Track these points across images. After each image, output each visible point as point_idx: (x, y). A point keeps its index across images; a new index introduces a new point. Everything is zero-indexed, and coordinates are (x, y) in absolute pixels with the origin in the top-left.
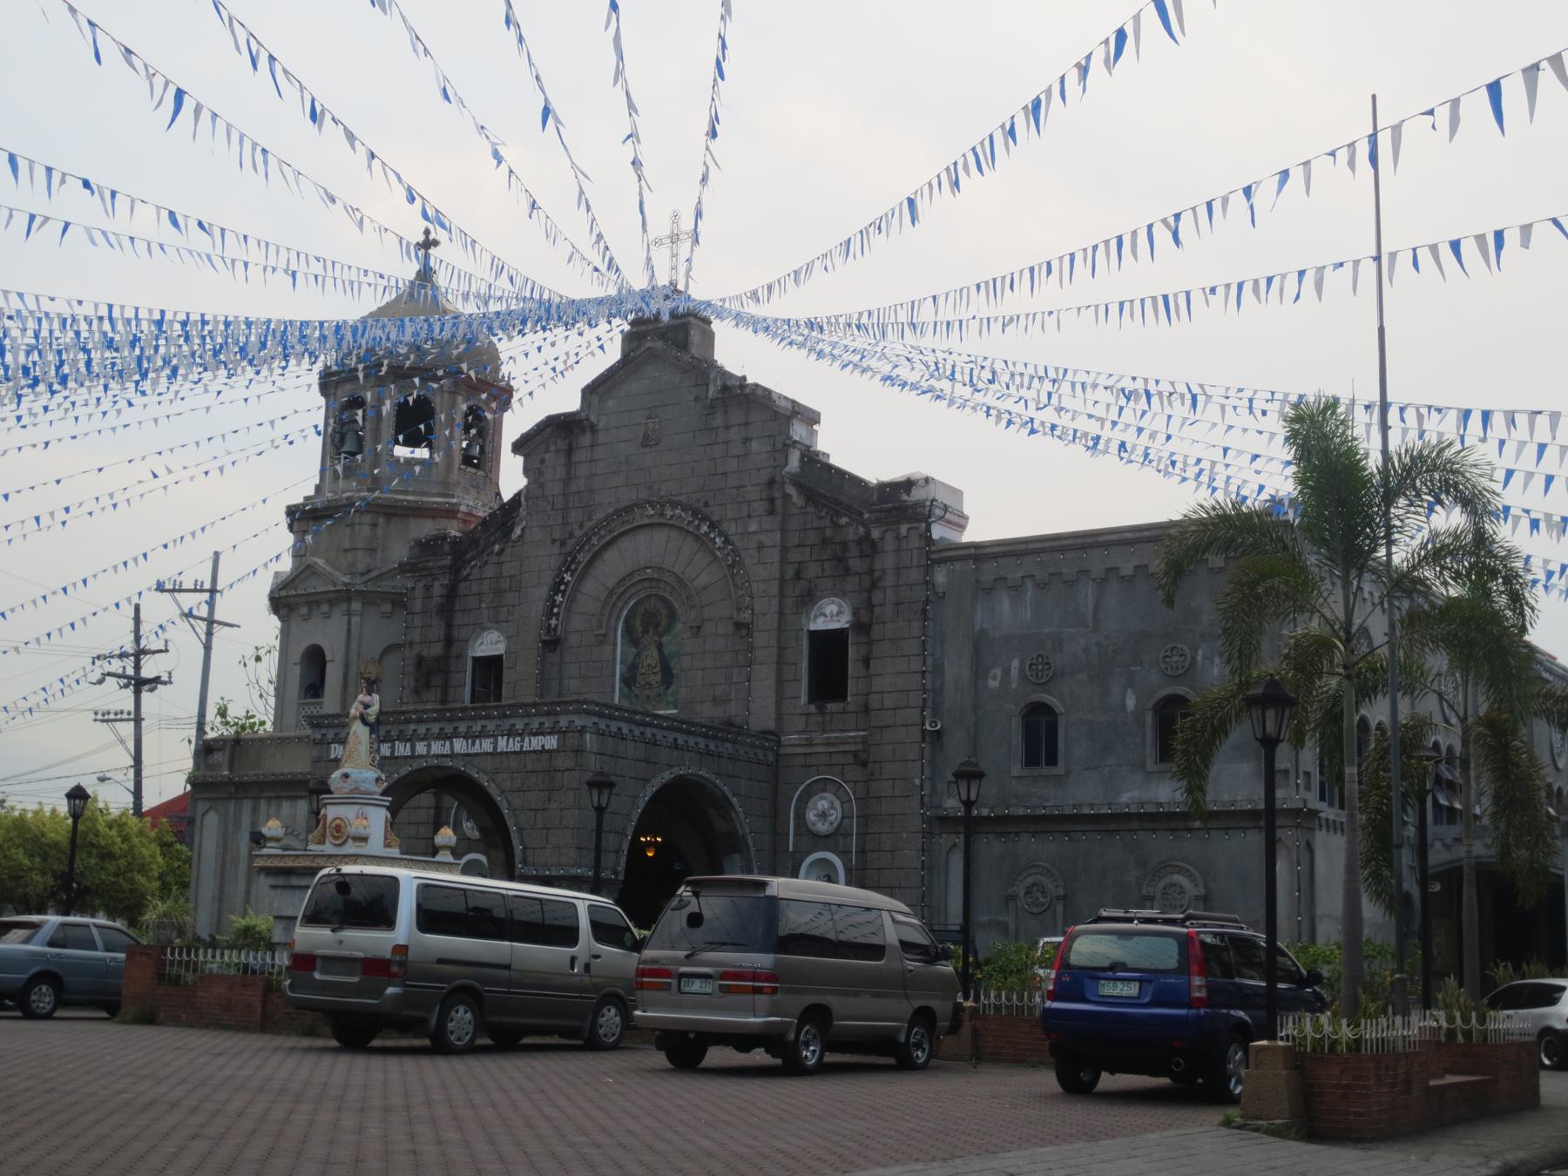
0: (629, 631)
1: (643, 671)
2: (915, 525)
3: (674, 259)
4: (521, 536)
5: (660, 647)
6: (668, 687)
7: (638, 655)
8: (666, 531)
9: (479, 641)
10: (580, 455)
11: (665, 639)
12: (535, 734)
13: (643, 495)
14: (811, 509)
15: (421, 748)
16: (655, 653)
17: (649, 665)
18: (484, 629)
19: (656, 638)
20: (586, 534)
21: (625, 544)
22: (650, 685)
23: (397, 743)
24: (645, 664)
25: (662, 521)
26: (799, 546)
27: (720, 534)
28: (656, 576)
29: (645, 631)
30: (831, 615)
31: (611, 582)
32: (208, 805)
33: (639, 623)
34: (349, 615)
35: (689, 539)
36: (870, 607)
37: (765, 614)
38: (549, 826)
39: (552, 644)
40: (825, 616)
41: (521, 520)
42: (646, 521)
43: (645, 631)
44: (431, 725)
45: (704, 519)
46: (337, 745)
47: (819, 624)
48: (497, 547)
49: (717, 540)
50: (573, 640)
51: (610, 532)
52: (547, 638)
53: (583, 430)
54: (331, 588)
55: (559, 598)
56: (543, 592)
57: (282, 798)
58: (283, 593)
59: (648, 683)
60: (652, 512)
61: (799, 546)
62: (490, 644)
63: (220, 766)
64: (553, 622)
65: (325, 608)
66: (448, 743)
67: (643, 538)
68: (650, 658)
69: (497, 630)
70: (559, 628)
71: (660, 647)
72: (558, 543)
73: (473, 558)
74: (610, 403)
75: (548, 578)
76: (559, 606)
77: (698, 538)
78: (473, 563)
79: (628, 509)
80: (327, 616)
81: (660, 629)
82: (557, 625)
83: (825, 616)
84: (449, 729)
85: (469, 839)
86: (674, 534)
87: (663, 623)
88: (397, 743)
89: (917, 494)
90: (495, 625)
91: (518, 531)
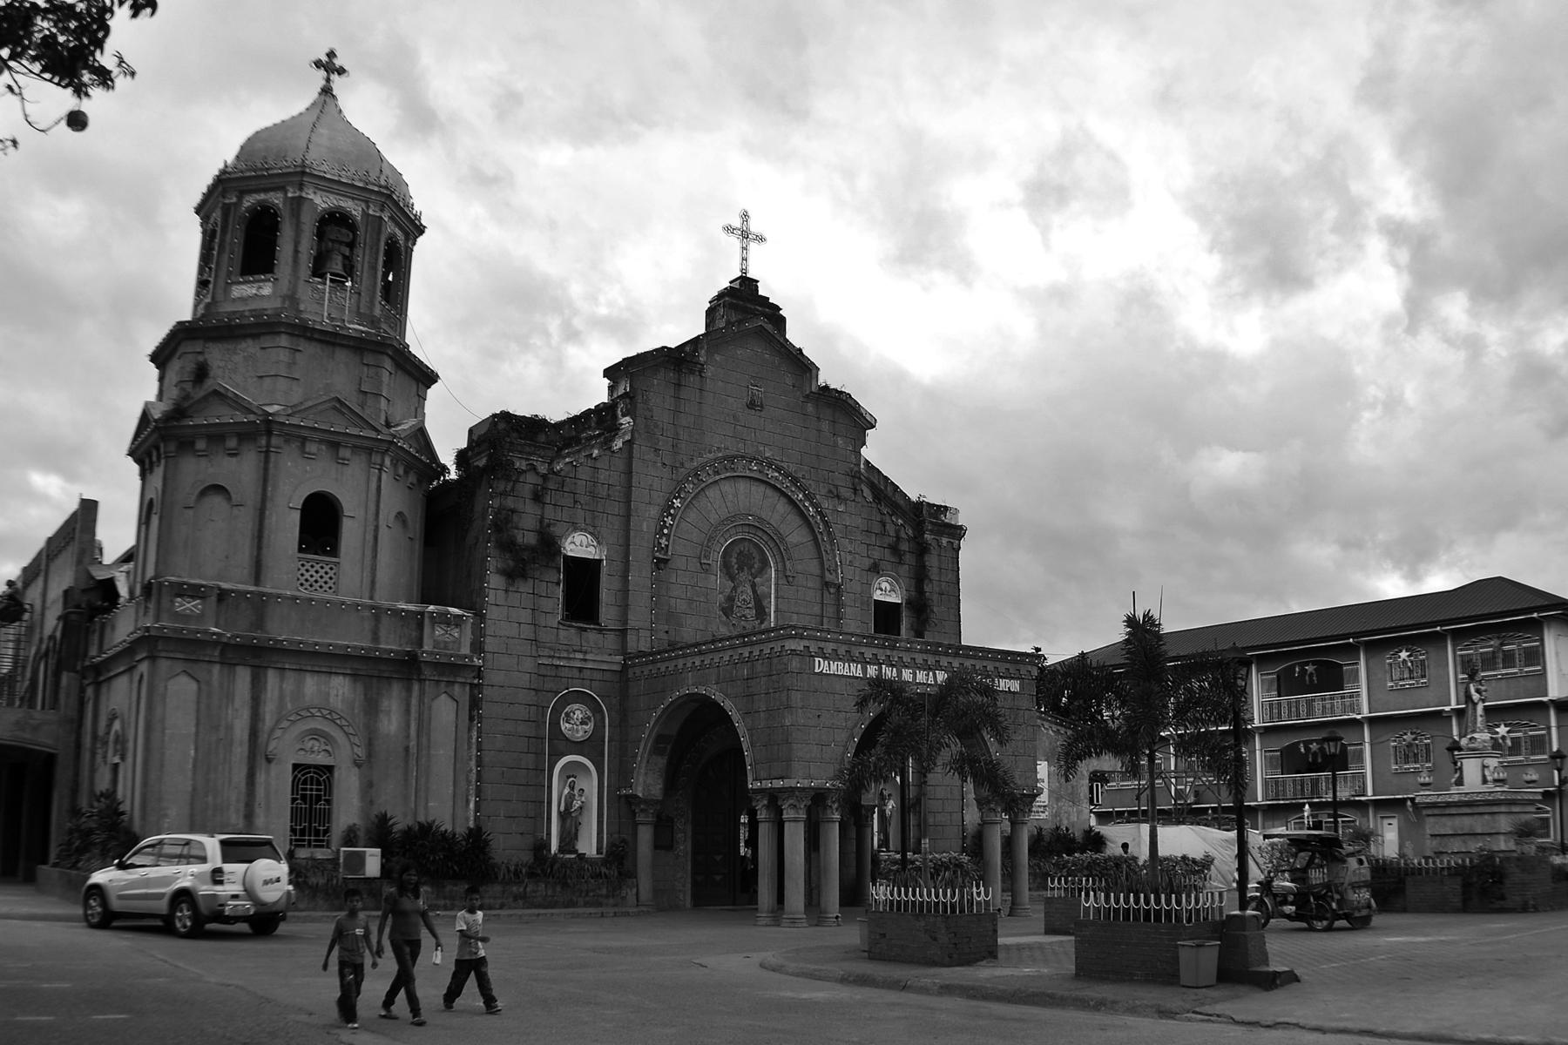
0: (726, 565)
1: (740, 604)
2: (952, 541)
3: (745, 252)
4: (620, 449)
5: (753, 586)
6: (762, 623)
7: (735, 588)
8: (762, 488)
9: (569, 540)
10: (684, 394)
11: (757, 580)
12: (1002, 677)
13: (750, 451)
14: (874, 505)
15: (907, 675)
16: (750, 591)
17: (744, 600)
18: (575, 530)
19: (750, 578)
20: (696, 469)
21: (727, 487)
22: (746, 618)
23: (884, 666)
24: (741, 598)
25: (765, 479)
26: (867, 531)
27: (812, 504)
28: (757, 524)
29: (741, 569)
30: (887, 591)
31: (714, 518)
32: (179, 667)
33: (735, 561)
34: (380, 470)
35: (783, 500)
36: (920, 590)
37: (851, 580)
38: (1016, 754)
39: (661, 564)
40: (882, 590)
41: (624, 434)
42: (748, 473)
43: (741, 569)
44: (916, 656)
45: (802, 489)
46: (821, 660)
47: (878, 596)
48: (596, 452)
49: (811, 509)
50: (679, 563)
51: (717, 473)
52: (661, 556)
53: (692, 372)
54: (373, 434)
55: (669, 521)
56: (654, 511)
57: (331, 673)
58: (294, 421)
59: (744, 616)
60: (755, 468)
61: (867, 531)
62: (578, 545)
63: (200, 617)
64: (663, 541)
65: (345, 453)
66: (931, 673)
67: (742, 486)
68: (746, 593)
69: (590, 533)
70: (670, 548)
71: (753, 586)
72: (668, 469)
73: (568, 455)
74: (718, 358)
75: (659, 498)
76: (667, 528)
77: (791, 501)
78: (567, 460)
79: (731, 459)
80: (343, 462)
81: (753, 571)
82: (667, 546)
83: (882, 590)
84: (931, 660)
85: (567, 739)
86: (769, 492)
87: (756, 566)
88: (884, 666)
89: (948, 519)
90: (591, 529)
91: (618, 444)
